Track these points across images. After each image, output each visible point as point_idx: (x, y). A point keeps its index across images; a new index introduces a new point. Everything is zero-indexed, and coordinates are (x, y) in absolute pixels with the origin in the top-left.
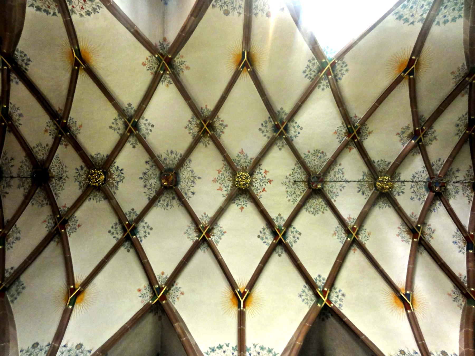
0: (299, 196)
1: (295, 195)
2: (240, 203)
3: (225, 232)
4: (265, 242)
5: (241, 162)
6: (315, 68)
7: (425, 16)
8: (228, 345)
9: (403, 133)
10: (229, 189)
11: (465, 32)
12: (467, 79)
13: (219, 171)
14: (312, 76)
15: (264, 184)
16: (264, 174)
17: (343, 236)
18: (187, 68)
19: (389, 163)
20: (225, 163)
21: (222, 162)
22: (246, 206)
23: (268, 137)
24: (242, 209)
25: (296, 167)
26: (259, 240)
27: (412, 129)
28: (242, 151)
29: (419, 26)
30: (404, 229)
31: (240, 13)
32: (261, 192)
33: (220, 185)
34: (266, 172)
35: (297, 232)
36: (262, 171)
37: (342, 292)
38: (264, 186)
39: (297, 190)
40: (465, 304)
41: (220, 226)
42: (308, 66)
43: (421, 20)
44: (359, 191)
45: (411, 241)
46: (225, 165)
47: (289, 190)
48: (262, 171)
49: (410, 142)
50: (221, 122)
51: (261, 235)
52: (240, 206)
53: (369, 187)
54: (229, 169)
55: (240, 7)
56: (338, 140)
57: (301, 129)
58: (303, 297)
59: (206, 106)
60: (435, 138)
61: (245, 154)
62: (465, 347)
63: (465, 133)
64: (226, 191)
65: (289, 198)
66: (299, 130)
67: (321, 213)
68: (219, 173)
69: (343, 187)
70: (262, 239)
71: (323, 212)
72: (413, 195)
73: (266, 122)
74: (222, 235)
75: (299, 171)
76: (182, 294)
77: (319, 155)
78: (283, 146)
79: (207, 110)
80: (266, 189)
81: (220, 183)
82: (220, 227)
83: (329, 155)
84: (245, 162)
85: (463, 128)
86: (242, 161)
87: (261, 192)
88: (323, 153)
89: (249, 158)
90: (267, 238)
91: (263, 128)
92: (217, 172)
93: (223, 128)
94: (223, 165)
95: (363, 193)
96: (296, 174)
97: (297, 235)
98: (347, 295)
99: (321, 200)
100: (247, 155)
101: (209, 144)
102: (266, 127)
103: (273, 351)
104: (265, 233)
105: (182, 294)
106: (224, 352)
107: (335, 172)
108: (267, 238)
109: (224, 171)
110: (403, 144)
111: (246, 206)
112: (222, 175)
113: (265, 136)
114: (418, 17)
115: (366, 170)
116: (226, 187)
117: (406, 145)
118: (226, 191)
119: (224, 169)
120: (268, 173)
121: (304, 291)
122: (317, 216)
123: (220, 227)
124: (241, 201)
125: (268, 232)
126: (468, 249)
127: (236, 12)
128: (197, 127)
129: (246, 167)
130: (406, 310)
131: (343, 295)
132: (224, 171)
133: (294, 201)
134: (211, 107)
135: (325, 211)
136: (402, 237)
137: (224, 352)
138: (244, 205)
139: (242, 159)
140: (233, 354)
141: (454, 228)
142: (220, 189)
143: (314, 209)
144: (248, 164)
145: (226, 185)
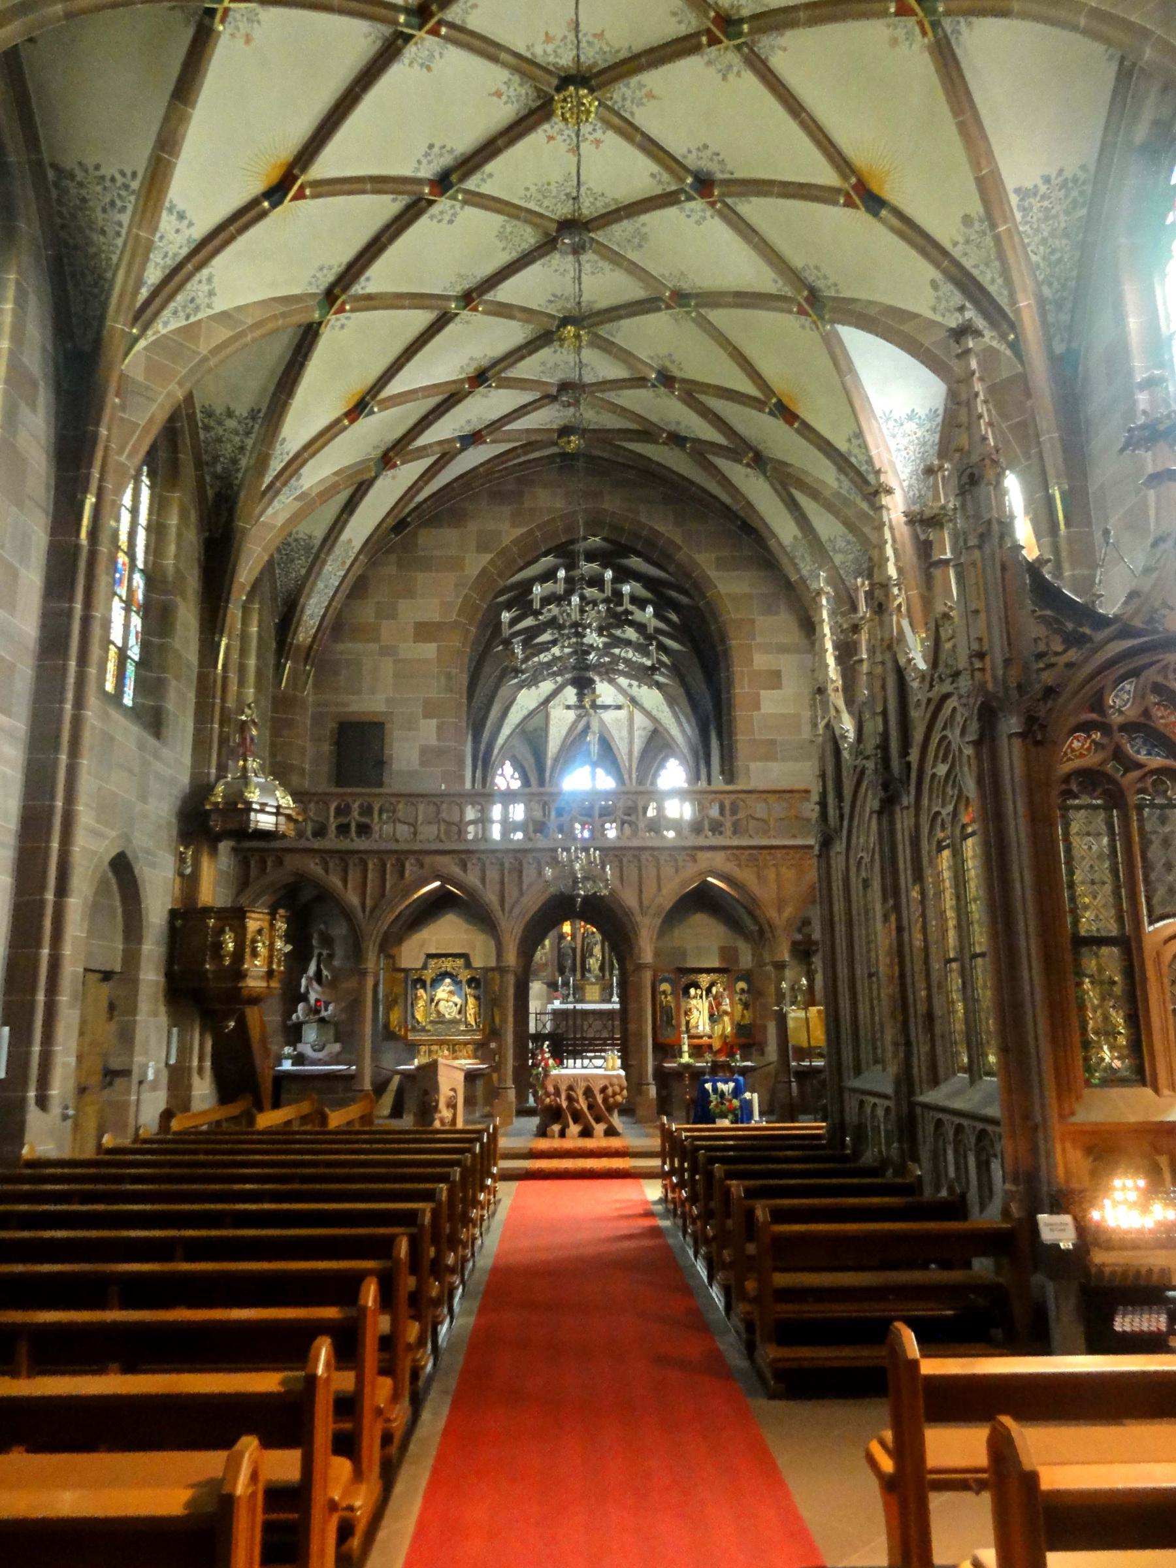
0: (540, 206)
1: (540, 197)
2: (512, 89)
3: (429, 69)
4: (419, 162)
5: (624, 89)
6: (820, 284)
7: (853, 460)
8: (191, 224)
9: (673, 362)
10: (551, 59)
11: (817, 480)
12: (751, 455)
13: (600, 36)
14: (806, 274)
15: (565, 137)
16: (591, 138)
17: (458, 290)
18: (894, 42)
19: (612, 335)
20: (624, 54)
21: (627, 45)
22: (506, 103)
23: (685, 157)
24: (498, 94)
25: (607, 200)
26: (424, 148)
27: (676, 373)
28: (653, 97)
29: (843, 446)
30: (485, 363)
31: (955, 244)
32: (545, 131)
33: (559, 37)
34: (598, 142)
35: (455, 215)
36: (599, 134)
37: (346, 322)
38: (559, 138)
39: (554, 201)
40: (372, 459)
41: (445, 52)
42: (825, 277)
43: (850, 452)
44: (554, 296)
45: (463, 376)
46: (618, 51)
47: (553, 187)
48: (599, 134)
49: (651, 367)
50: (735, 69)
51: (436, 150)
52: (504, 88)
53: (564, 308)
54: (605, 61)
55: (966, 254)
56: (667, 274)
57: (698, 223)
58: (319, 275)
59: (785, 50)
60: (657, 396)
61: (645, 100)
62: (317, 495)
63: (664, 430)
64: (545, 51)
65: (533, 189)
66: (695, 217)
67: (502, 245)
68: (595, 35)
69: (562, 274)
70: (427, 155)
71: (504, 249)
72: (550, 364)
73: (722, 162)
74: (422, 65)
75: (599, 204)
76: (248, 39)
77: (636, 241)
78: (660, 182)
79: (772, 47)
80: (552, 142)
81: (565, 37)
82: (441, 54)
83: (632, 255)
84: (624, 99)
85: (672, 428)
86: (628, 93)
87: (545, 131)
88: (640, 246)
89: (635, 109)
90: (429, 162)
91: (709, 153)
92: (599, 32)
93: (719, 67)
94: (617, 47)
95: (550, 302)
96: (592, 200)
97: (447, 217)
98: (345, 331)
99: (532, 241)
100: (642, 104)
101: (680, 22)
102: (711, 160)
103: (214, 299)
104: (441, 155)
105: (248, 39)
106: (177, 231)
107: (596, 262)
108: (429, 162)
109: (601, 49)
110: (651, 358)
111: (506, 103)
112: (588, 42)
113: (690, 151)
114: (856, 451)
115: (603, 303)
116: (555, 52)
117: (649, 361)
118: (545, 51)
119: (606, 49)
120: (594, 146)
121: (330, 268)
122: (497, 242)
123: (441, 54)
124: (519, 89)
125: (447, 161)
126: (462, 438)
127: (961, 240)
128: (732, 6)
129: (611, 98)
130: (347, 414)
131: (342, 327)
132: (601, 49)
133: (528, 199)
134: (779, 62)
135: (508, 251)
136: (468, 365)
137: (177, 231)
138: (509, 97)
139: (634, 92)
140: (181, 247)
141: (495, 416)
142: (548, 38)
143: (511, 233)
144: (620, 104)
145: (559, 51)
